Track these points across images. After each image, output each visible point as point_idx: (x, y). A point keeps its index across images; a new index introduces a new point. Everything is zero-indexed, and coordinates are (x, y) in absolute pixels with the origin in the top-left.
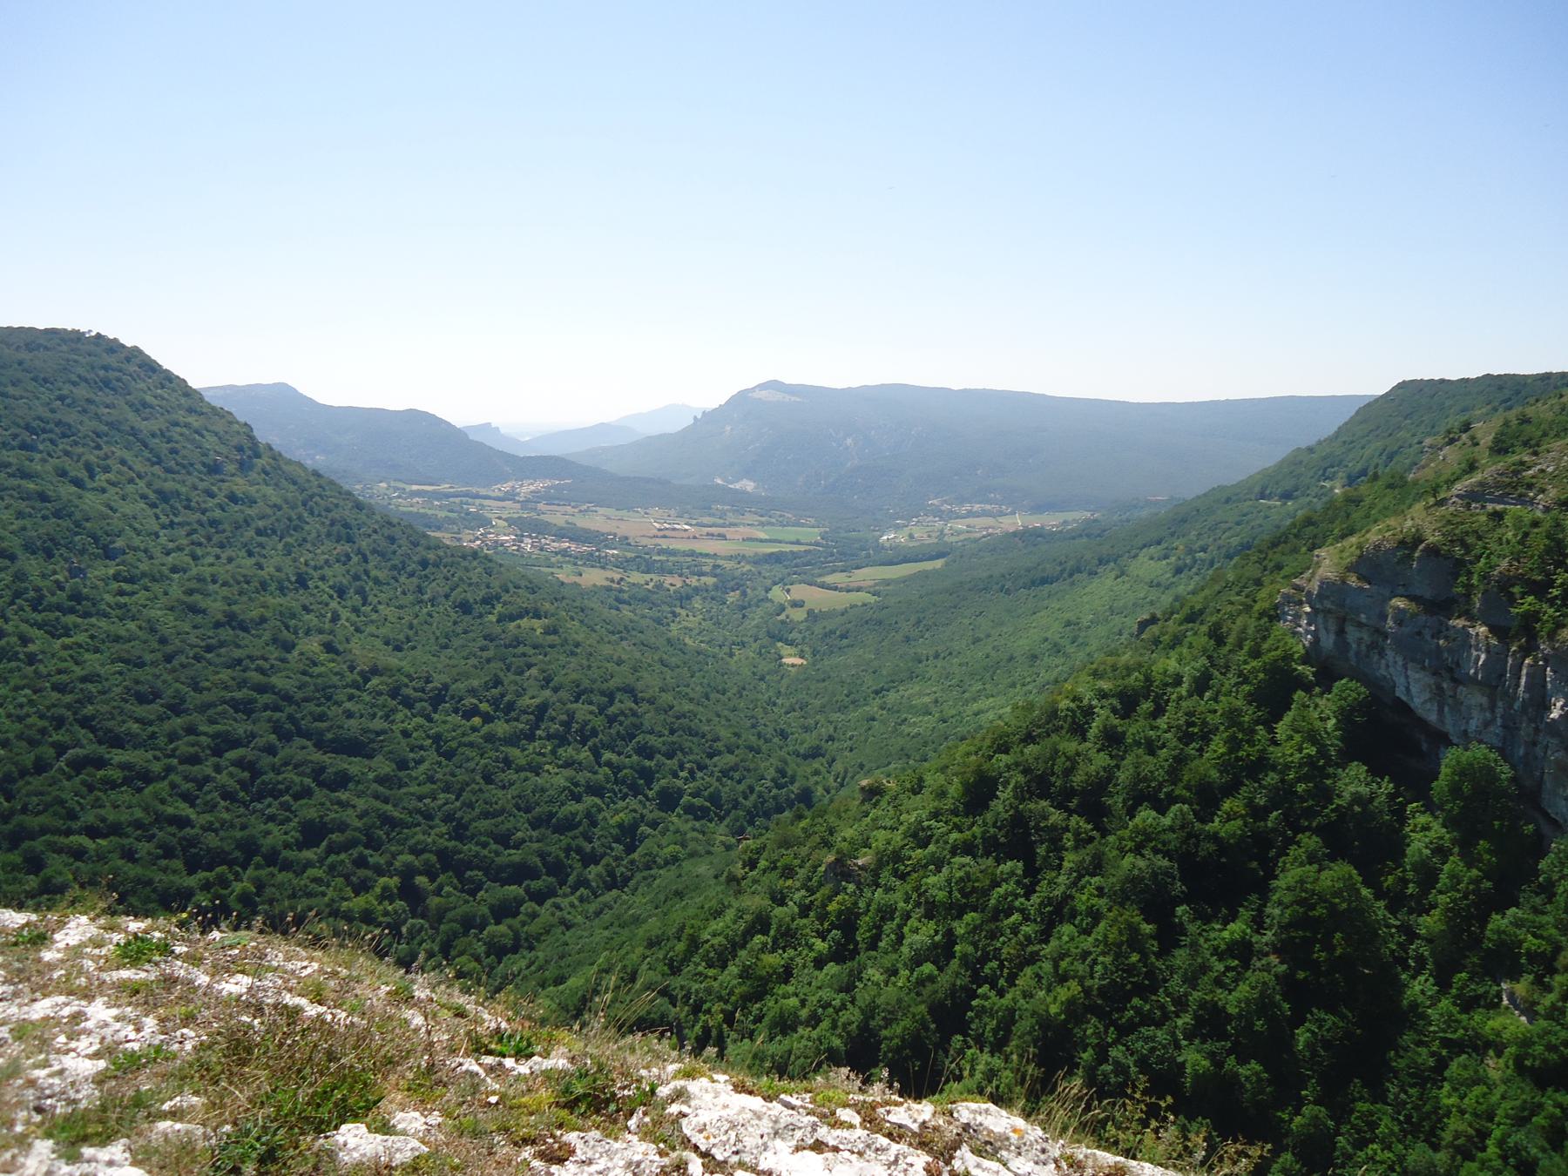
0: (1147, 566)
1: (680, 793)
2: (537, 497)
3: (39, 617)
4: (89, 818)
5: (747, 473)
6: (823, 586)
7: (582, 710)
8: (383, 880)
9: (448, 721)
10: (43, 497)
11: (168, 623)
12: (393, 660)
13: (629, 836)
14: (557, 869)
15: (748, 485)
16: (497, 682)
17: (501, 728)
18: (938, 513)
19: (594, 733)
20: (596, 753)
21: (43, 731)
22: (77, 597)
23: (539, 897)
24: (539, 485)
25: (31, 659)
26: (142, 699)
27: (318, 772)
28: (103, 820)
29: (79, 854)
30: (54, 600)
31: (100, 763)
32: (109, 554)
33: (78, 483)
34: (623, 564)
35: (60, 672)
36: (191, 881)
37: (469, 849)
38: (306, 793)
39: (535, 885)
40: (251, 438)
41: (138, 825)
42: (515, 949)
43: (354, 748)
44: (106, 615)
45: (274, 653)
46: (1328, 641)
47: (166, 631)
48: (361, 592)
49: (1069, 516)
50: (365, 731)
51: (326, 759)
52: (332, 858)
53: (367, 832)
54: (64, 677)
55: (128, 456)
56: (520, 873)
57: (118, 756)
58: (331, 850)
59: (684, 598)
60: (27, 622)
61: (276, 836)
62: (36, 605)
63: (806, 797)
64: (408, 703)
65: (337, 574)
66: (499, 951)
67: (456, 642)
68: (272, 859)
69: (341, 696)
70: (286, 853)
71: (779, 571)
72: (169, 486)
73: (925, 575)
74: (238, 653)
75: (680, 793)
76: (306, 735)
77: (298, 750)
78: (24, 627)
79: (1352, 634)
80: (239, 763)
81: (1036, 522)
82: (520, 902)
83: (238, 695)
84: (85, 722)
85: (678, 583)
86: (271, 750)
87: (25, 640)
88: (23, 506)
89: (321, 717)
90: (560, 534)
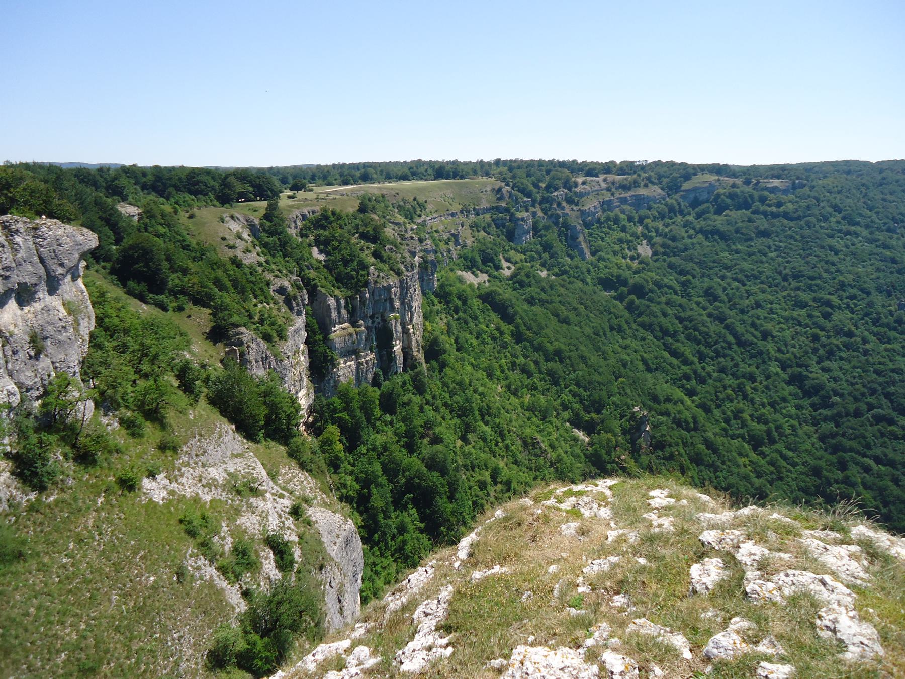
3: (875, 330)
4: (878, 451)
21: (863, 394)
25: (866, 352)
28: (886, 455)
29: (867, 470)
30: (886, 321)
31: (891, 422)
35: (880, 363)
54: (882, 367)
60: (868, 331)
62: (876, 322)
78: (866, 334)
84: (888, 396)
88: (881, 264)
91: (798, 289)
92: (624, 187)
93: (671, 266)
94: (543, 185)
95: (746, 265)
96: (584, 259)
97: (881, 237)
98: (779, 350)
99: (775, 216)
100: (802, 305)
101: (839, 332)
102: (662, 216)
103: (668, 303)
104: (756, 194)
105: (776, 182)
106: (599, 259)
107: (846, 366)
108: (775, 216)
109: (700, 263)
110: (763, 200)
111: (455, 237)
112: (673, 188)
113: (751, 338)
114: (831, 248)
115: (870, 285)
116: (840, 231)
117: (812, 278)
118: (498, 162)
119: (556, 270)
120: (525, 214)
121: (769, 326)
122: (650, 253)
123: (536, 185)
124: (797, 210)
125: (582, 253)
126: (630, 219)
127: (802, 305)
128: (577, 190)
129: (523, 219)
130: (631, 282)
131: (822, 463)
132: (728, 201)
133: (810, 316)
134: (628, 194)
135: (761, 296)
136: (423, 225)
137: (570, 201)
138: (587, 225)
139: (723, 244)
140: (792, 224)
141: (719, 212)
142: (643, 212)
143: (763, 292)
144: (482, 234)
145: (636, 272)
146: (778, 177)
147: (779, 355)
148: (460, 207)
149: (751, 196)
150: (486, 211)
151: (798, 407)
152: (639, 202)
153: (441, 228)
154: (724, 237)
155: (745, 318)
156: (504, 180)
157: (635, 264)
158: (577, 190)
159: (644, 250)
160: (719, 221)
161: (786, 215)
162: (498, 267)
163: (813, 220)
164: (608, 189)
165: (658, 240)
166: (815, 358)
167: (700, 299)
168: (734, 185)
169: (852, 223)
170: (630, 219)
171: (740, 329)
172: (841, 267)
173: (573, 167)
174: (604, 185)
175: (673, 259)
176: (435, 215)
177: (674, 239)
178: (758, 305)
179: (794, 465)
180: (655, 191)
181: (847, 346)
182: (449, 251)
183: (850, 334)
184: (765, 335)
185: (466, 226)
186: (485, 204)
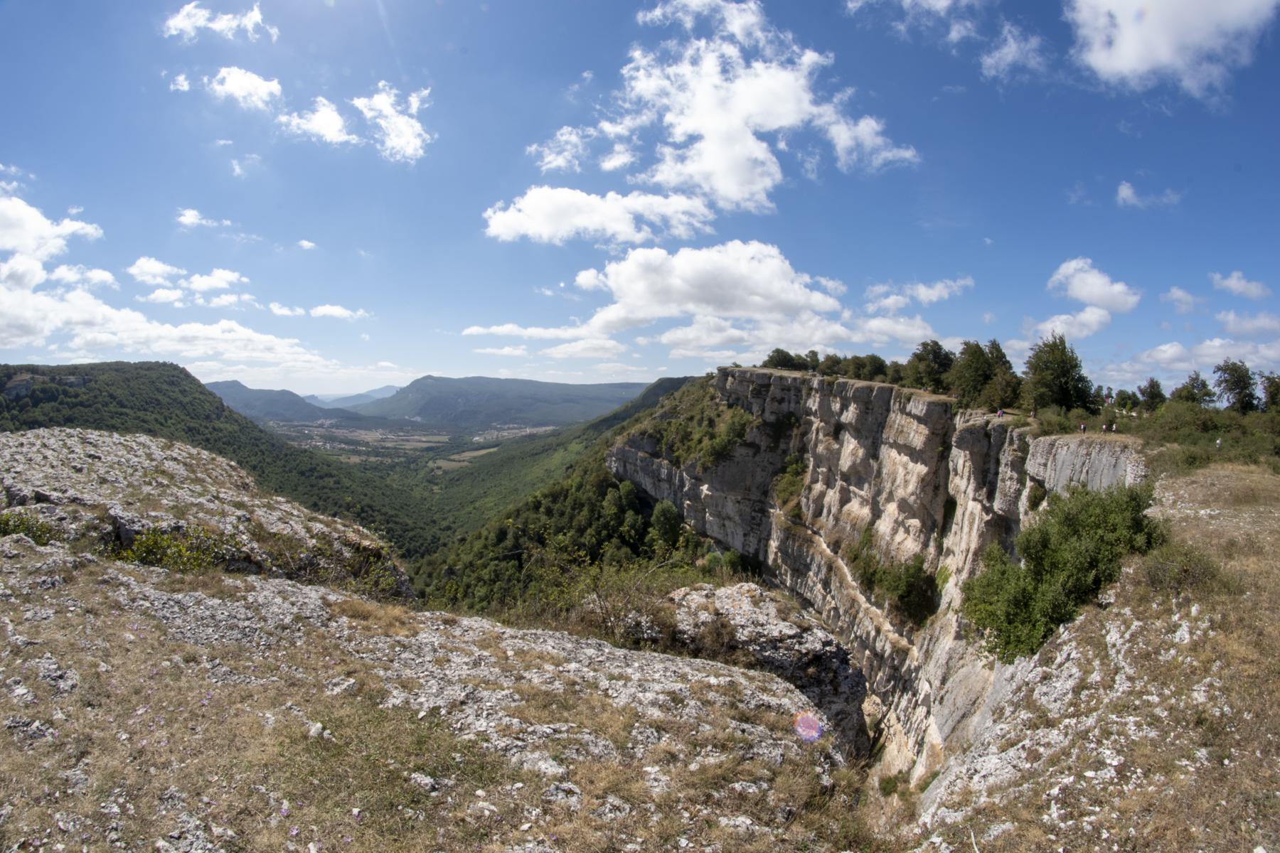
0: (575, 447)
2: (332, 426)
5: (419, 414)
15: (418, 419)
33: (162, 424)
34: (368, 454)
40: (222, 405)
46: (621, 470)
49: (548, 428)
59: (392, 467)
71: (431, 454)
72: (192, 425)
73: (490, 454)
79: (628, 466)
81: (535, 430)
85: (390, 461)
90: (341, 442)
97: (141, 414)
99: (75, 405)
104: (60, 388)
108: (75, 405)
110: (65, 393)
116: (116, 413)
124: (88, 400)
132: (41, 395)
140: (86, 410)
141: (35, 405)
149: (57, 390)
161: (81, 404)
163: (99, 406)
168: (44, 383)
169: (123, 406)
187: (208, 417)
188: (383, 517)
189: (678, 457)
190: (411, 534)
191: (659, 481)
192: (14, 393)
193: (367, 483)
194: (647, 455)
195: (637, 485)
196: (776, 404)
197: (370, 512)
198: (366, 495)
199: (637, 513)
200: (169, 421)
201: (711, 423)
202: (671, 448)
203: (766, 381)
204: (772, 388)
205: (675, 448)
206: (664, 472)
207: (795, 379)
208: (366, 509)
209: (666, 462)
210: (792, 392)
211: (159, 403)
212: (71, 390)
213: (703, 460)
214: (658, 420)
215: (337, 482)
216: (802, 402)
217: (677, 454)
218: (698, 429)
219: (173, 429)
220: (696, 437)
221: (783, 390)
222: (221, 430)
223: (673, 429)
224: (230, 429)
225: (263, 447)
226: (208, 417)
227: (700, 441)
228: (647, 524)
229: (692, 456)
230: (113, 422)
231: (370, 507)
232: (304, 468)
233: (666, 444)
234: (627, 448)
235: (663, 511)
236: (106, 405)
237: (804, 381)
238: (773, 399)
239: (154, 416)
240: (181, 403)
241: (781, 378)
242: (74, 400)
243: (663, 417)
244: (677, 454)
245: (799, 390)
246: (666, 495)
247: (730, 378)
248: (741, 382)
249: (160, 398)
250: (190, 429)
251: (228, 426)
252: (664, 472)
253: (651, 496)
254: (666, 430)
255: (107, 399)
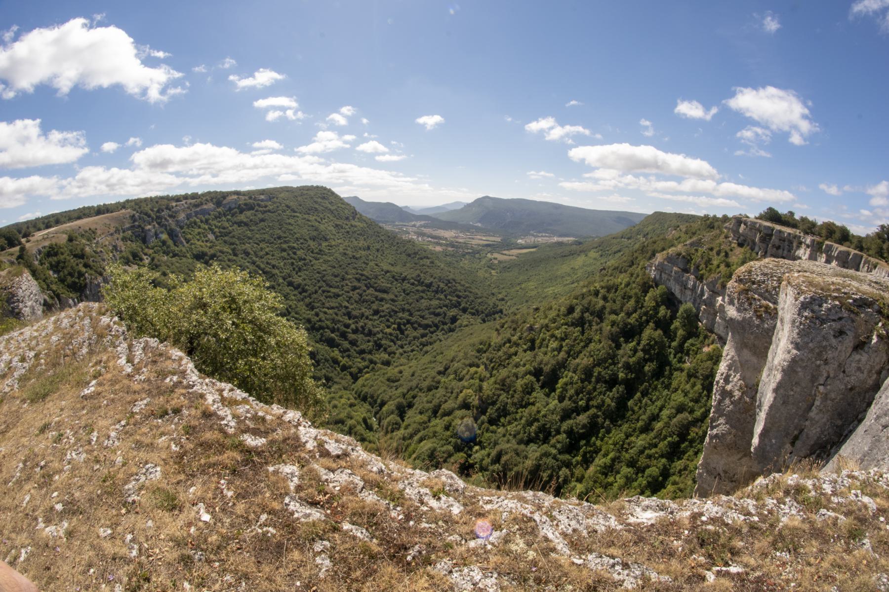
1: (468, 308)
3: (313, 255)
6: (502, 254)
7: (442, 285)
8: (394, 326)
9: (406, 285)
10: (313, 226)
11: (340, 258)
12: (392, 269)
13: (454, 320)
14: (437, 326)
16: (419, 276)
17: (420, 288)
18: (533, 235)
19: (445, 291)
20: (446, 296)
22: (320, 250)
23: (432, 333)
24: (422, 223)
25: (312, 266)
26: (336, 276)
27: (376, 297)
32: (326, 240)
33: (319, 222)
36: (351, 322)
37: (413, 319)
38: (373, 302)
39: (432, 330)
41: (337, 307)
42: (427, 345)
43: (385, 291)
44: (326, 255)
45: (364, 266)
47: (339, 259)
48: (382, 250)
50: (387, 287)
51: (377, 293)
52: (381, 319)
53: (389, 313)
55: (329, 215)
56: (426, 327)
57: (333, 290)
58: (381, 317)
61: (367, 313)
62: (312, 252)
63: (501, 311)
64: (396, 280)
65: (378, 246)
66: (424, 345)
67: (408, 265)
68: (367, 318)
69: (380, 277)
70: (370, 317)
74: (356, 266)
75: (468, 308)
76: (373, 287)
77: (371, 291)
80: (358, 293)
82: (427, 334)
83: (357, 276)
86: (365, 291)
87: (311, 261)
88: (310, 228)
89: (376, 283)
91: (281, 243)
92: (196, 206)
93: (225, 242)
94: (155, 209)
95: (257, 236)
96: (184, 246)
97: (306, 216)
98: (281, 272)
99: (265, 212)
100: (284, 250)
101: (301, 259)
102: (216, 217)
103: (229, 260)
104: (255, 203)
105: (262, 197)
106: (192, 244)
107: (307, 273)
108: (265, 212)
109: (239, 238)
110: (259, 205)
111: (115, 247)
112: (218, 204)
113: (269, 270)
114: (290, 224)
115: (307, 238)
117: (285, 237)
118: (128, 201)
119: (171, 254)
120: (148, 227)
121: (273, 262)
122: (214, 238)
123: (152, 210)
125: (182, 243)
126: (202, 222)
127: (284, 250)
128: (173, 210)
129: (149, 230)
130: (209, 253)
131: (310, 316)
132: (244, 207)
133: (289, 254)
134: (198, 209)
135: (267, 250)
136: (97, 243)
137: (170, 216)
138: (182, 228)
139: (245, 228)
140: (272, 215)
141: (241, 212)
142: (207, 216)
143: (268, 247)
144: (129, 242)
145: (210, 248)
146: (263, 194)
147: (281, 275)
148: (114, 229)
150: (128, 229)
151: (294, 295)
152: (205, 212)
153: (107, 243)
154: (246, 224)
155: (263, 260)
156: (134, 210)
157: (208, 244)
158: (173, 210)
159: (211, 237)
160: (242, 217)
161: (269, 211)
162: (141, 260)
163: (281, 212)
164: (188, 208)
165: (216, 230)
166: (295, 272)
167: (243, 256)
168: (245, 200)
169: (295, 212)
170: (202, 222)
171: (262, 266)
172: (295, 231)
173: (168, 198)
174: (186, 206)
175: (226, 238)
176: (103, 236)
177: (224, 228)
178: (267, 254)
179: (301, 320)
180: (211, 206)
181: (305, 265)
182: (114, 256)
183: (305, 259)
184: (274, 267)
185: (120, 240)
186: (127, 225)
187: (347, 218)
188: (462, 288)
189: (702, 275)
190: (480, 300)
191: (685, 289)
192: (228, 206)
193: (449, 264)
194: (679, 270)
195: (669, 289)
196: (775, 249)
197: (454, 283)
198: (450, 272)
199: (667, 308)
200: (324, 221)
201: (727, 255)
202: (697, 267)
203: (770, 232)
204: (773, 237)
205: (700, 268)
206: (691, 284)
207: (789, 234)
208: (451, 281)
209: (692, 277)
210: (786, 243)
211: (316, 210)
212: (262, 203)
213: (722, 280)
214: (688, 246)
215: (432, 262)
216: (792, 252)
217: (701, 272)
218: (716, 257)
219: (326, 225)
220: (715, 263)
221: (780, 240)
222: (356, 226)
223: (699, 254)
224: (362, 226)
225: (382, 238)
226: (347, 218)
227: (718, 266)
228: (673, 317)
229: (712, 275)
230: (290, 221)
231: (454, 280)
232: (410, 252)
233: (694, 264)
234: (666, 263)
235: (686, 311)
236: (284, 211)
237: (795, 237)
238: (773, 246)
239: (314, 217)
240: (330, 210)
241: (780, 231)
242: (264, 209)
243: (692, 244)
244: (701, 272)
245: (791, 242)
246: (688, 299)
247: (742, 225)
248: (751, 229)
249: (317, 206)
250: (337, 225)
251: (359, 224)
252: (691, 284)
253: (676, 298)
254: (693, 254)
255: (285, 208)
